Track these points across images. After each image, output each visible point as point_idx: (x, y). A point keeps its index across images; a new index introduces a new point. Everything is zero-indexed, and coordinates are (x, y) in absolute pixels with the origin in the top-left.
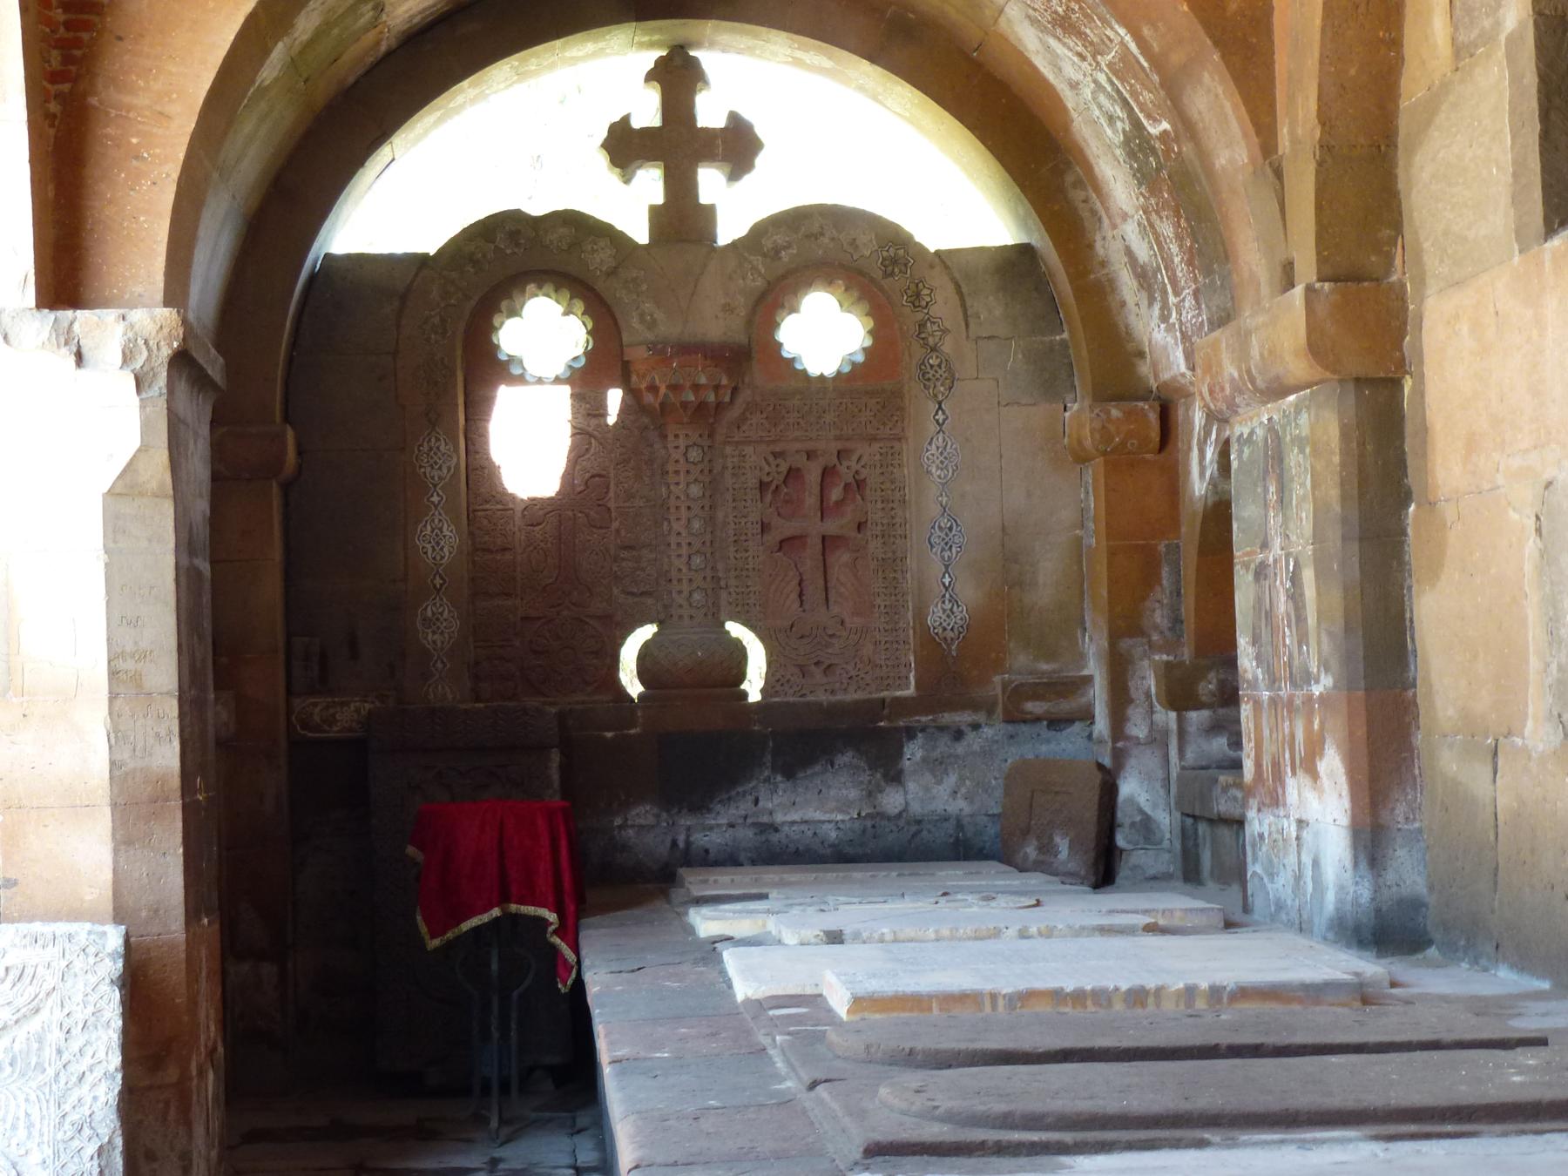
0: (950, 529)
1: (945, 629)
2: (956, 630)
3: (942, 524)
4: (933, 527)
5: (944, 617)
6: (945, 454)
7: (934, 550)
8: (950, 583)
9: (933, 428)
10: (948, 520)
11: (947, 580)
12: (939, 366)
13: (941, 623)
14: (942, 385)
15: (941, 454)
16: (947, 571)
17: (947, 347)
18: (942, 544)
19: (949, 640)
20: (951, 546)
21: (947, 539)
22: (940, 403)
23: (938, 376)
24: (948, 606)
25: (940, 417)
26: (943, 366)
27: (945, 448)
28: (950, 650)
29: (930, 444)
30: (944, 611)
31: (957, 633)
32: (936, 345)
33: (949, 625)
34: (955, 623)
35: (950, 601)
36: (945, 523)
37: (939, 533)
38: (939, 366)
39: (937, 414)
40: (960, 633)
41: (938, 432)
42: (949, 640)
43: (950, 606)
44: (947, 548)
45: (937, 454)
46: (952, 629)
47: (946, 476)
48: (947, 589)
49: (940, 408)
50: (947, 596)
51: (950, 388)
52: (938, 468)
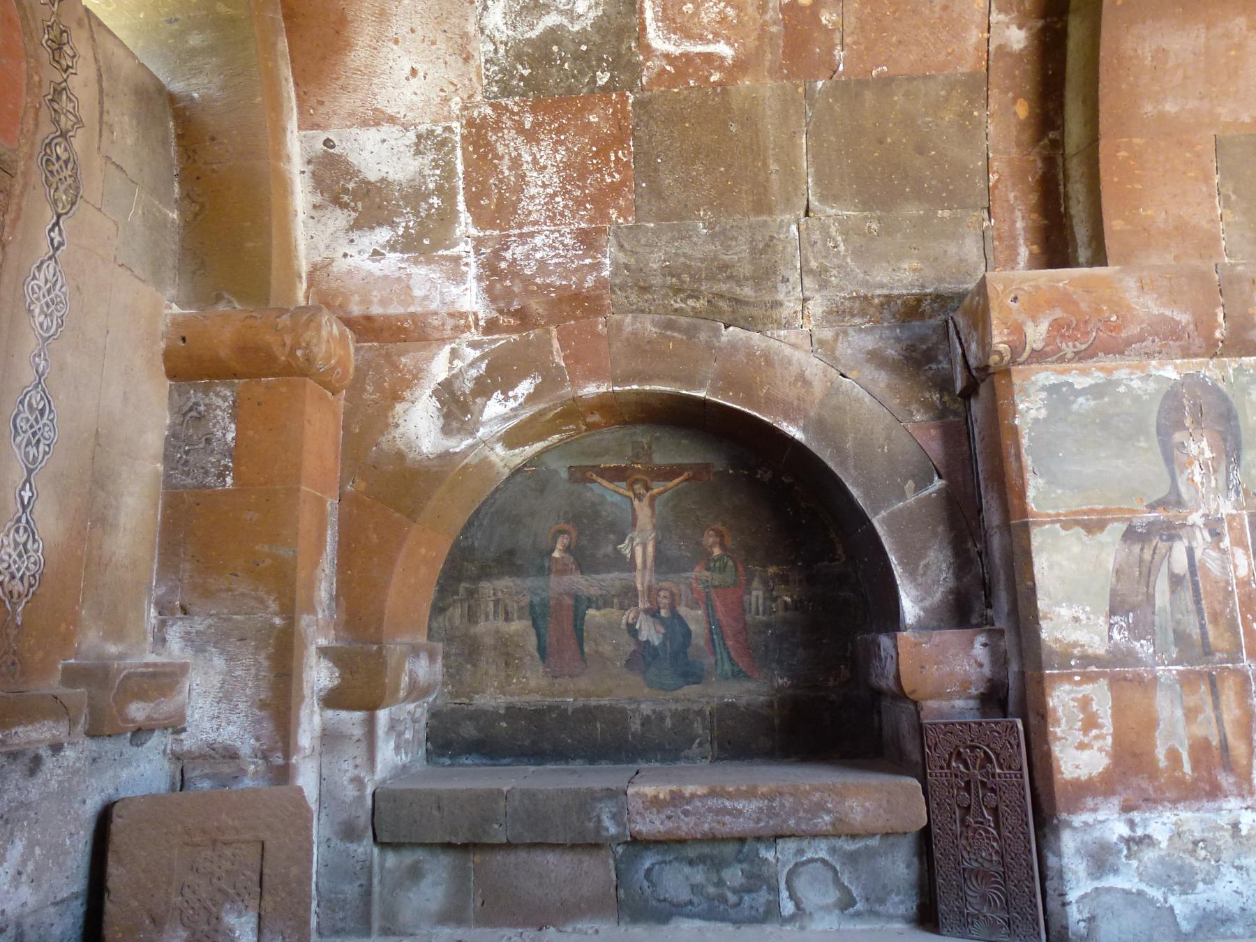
0: (42, 412)
1: (13, 577)
2: (25, 580)
3: (33, 401)
4: (22, 402)
5: (15, 556)
6: (53, 295)
7: (19, 439)
8: (30, 498)
9: (45, 249)
10: (42, 398)
11: (26, 494)
12: (66, 162)
13: (9, 566)
14: (65, 192)
15: (49, 292)
16: (28, 480)
17: (77, 143)
18: (30, 432)
19: (16, 595)
20: (39, 441)
21: (36, 427)
22: (59, 216)
23: (62, 176)
24: (22, 538)
25: (55, 234)
26: (70, 166)
27: (55, 284)
28: (14, 610)
29: (39, 268)
30: (16, 544)
31: (26, 584)
32: (68, 131)
33: (18, 570)
34: (27, 568)
35: (25, 530)
36: (36, 399)
37: (27, 414)
38: (66, 162)
39: (52, 230)
40: (31, 586)
41: (50, 258)
42: (16, 595)
43: (22, 538)
44: (34, 442)
45: (44, 290)
46: (22, 579)
47: (49, 329)
48: (24, 507)
49: (57, 223)
50: (24, 520)
51: (73, 204)
52: (42, 311)
